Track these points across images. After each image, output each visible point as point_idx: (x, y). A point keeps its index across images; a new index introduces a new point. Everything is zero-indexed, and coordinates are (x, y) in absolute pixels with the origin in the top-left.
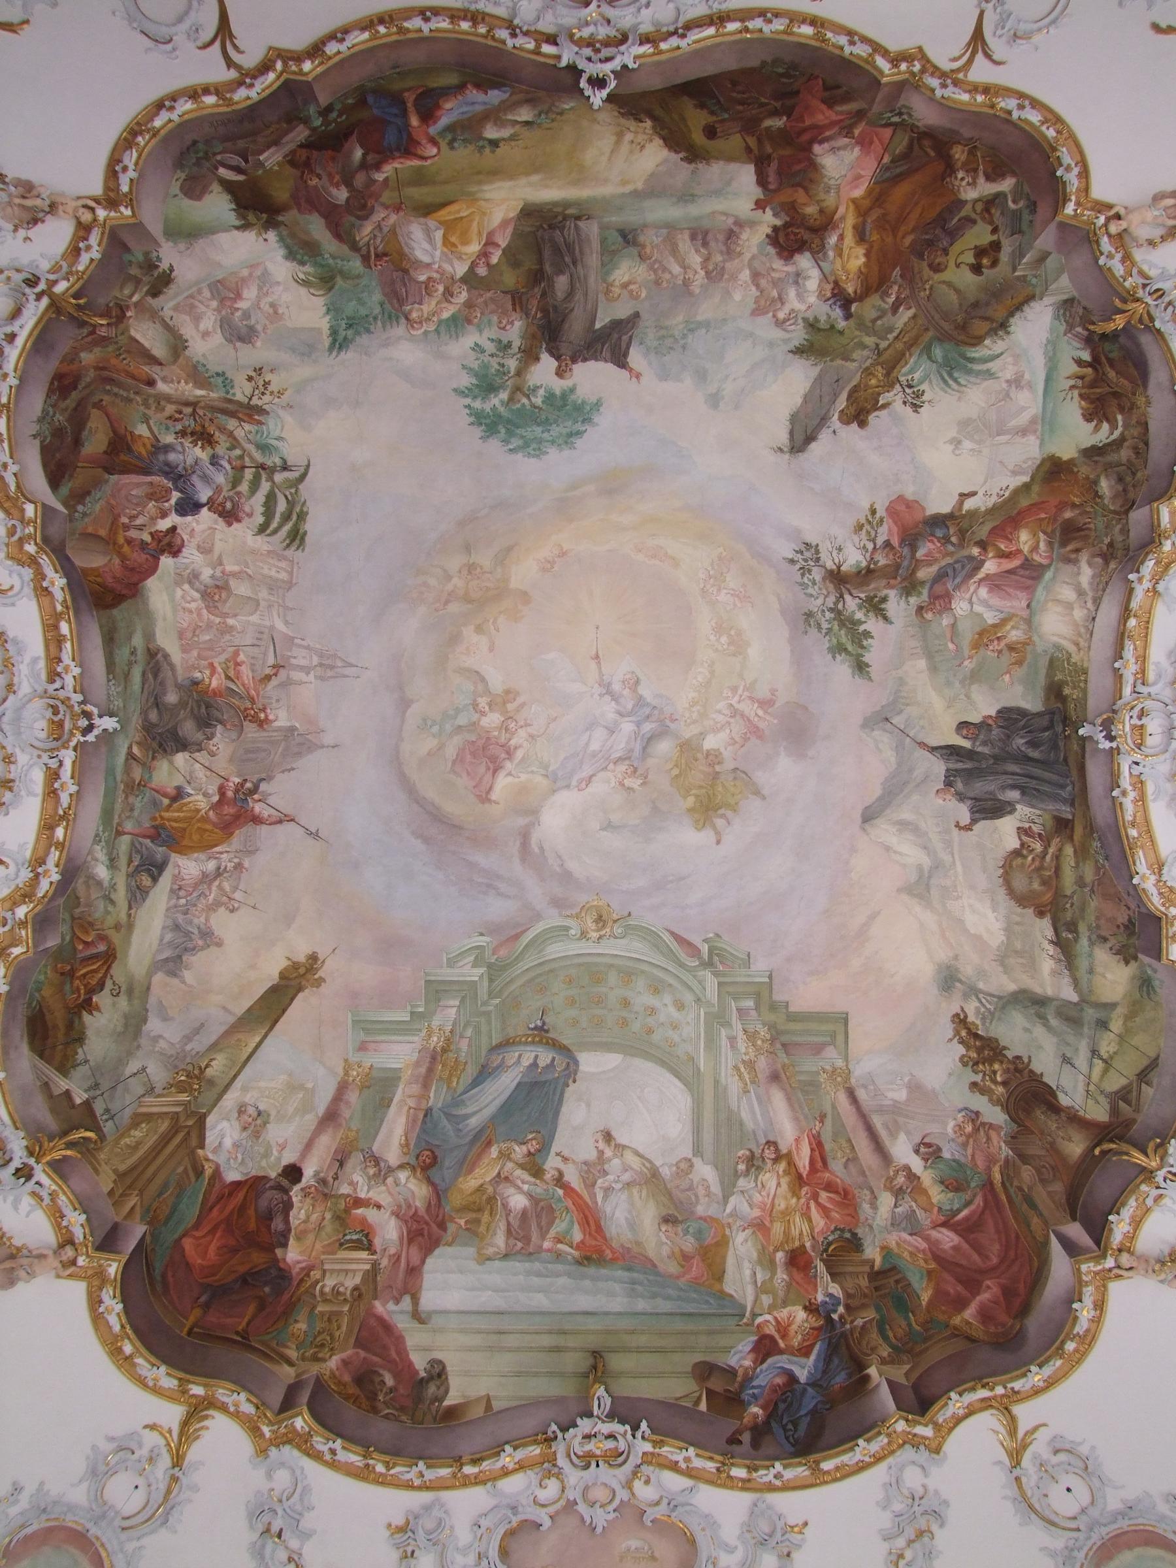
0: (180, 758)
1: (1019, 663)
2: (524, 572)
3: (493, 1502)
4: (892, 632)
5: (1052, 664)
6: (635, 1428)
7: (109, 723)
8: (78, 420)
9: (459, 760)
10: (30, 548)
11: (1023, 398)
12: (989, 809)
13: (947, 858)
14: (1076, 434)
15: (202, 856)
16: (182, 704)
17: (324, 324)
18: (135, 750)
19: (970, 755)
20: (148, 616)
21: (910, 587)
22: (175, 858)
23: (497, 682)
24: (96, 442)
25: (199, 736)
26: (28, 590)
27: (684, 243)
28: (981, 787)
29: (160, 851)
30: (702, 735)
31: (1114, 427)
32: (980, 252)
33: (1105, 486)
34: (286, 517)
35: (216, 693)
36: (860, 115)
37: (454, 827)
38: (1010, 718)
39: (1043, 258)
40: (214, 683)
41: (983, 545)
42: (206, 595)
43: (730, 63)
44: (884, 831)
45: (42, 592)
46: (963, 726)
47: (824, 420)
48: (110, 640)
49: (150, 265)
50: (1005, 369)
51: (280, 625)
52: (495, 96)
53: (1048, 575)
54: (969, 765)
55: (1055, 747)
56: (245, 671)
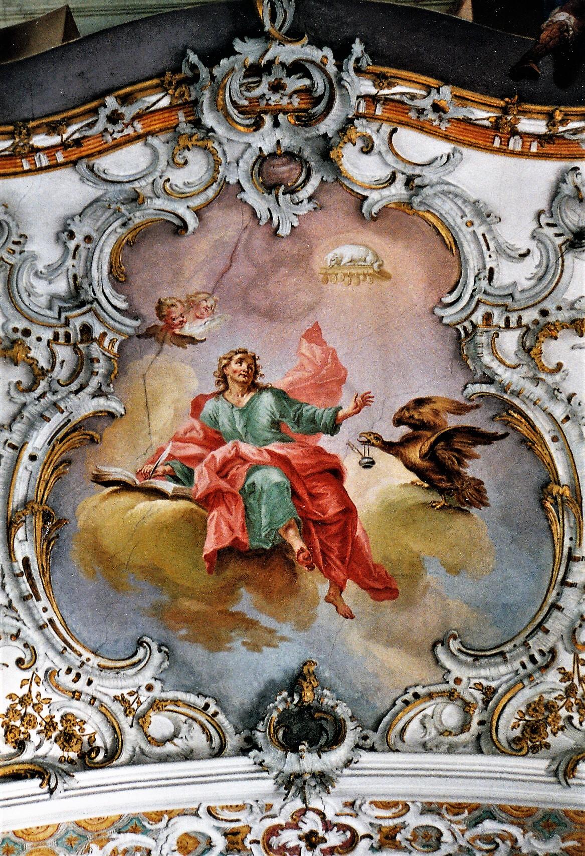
3: (91, 191)
6: (342, 53)
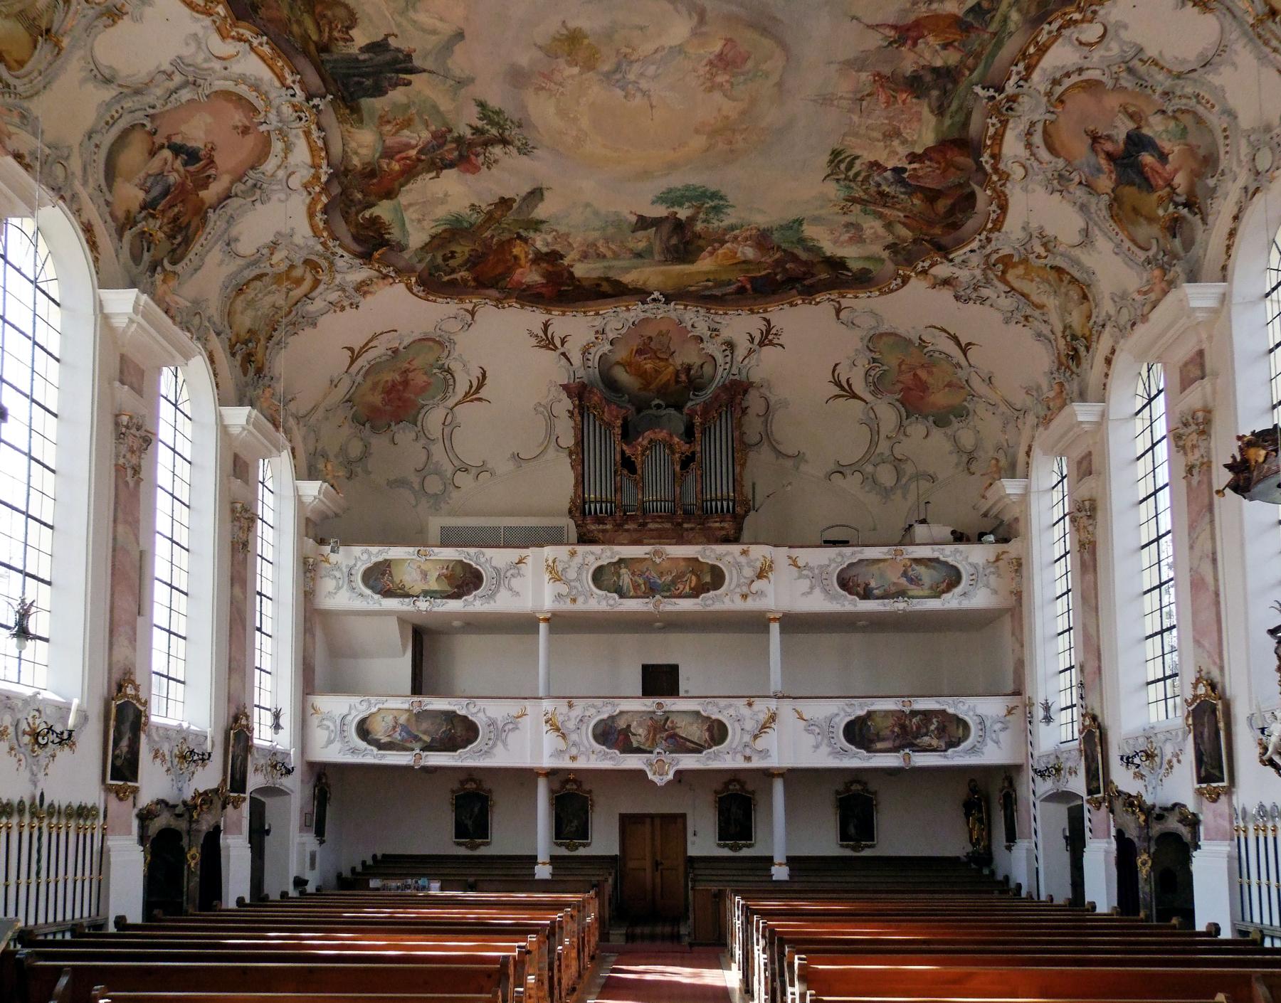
0: (938, 63)
1: (381, 117)
2: (698, 142)
4: (465, 121)
5: (361, 121)
7: (978, 89)
8: (951, 211)
9: (745, 60)
10: (995, 178)
11: (415, 216)
12: (377, 47)
13: (399, 19)
14: (383, 210)
15: (940, 12)
16: (929, 89)
17: (805, 227)
18: (967, 73)
19: (398, 71)
20: (937, 130)
21: (459, 140)
22: (961, 14)
23: (717, 96)
24: (942, 205)
25: (922, 73)
26: (1004, 159)
27: (609, 254)
28: (388, 57)
29: (969, 19)
30: (581, 73)
31: (363, 218)
32: (453, 257)
33: (359, 196)
34: (841, 161)
35: (902, 91)
36: (524, 290)
37: (752, 26)
38: (379, 91)
39: (420, 261)
40: (904, 96)
41: (419, 160)
42: (898, 134)
43: (590, 303)
44: (447, 29)
45: (996, 157)
46: (409, 83)
47: (524, 199)
48: (965, 124)
49: (896, 253)
50: (427, 224)
51: (855, 118)
52: (707, 293)
53: (377, 155)
54: (398, 66)
55: (345, 86)
56: (882, 98)
